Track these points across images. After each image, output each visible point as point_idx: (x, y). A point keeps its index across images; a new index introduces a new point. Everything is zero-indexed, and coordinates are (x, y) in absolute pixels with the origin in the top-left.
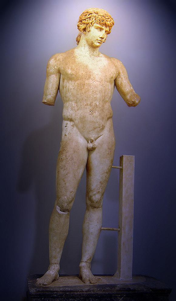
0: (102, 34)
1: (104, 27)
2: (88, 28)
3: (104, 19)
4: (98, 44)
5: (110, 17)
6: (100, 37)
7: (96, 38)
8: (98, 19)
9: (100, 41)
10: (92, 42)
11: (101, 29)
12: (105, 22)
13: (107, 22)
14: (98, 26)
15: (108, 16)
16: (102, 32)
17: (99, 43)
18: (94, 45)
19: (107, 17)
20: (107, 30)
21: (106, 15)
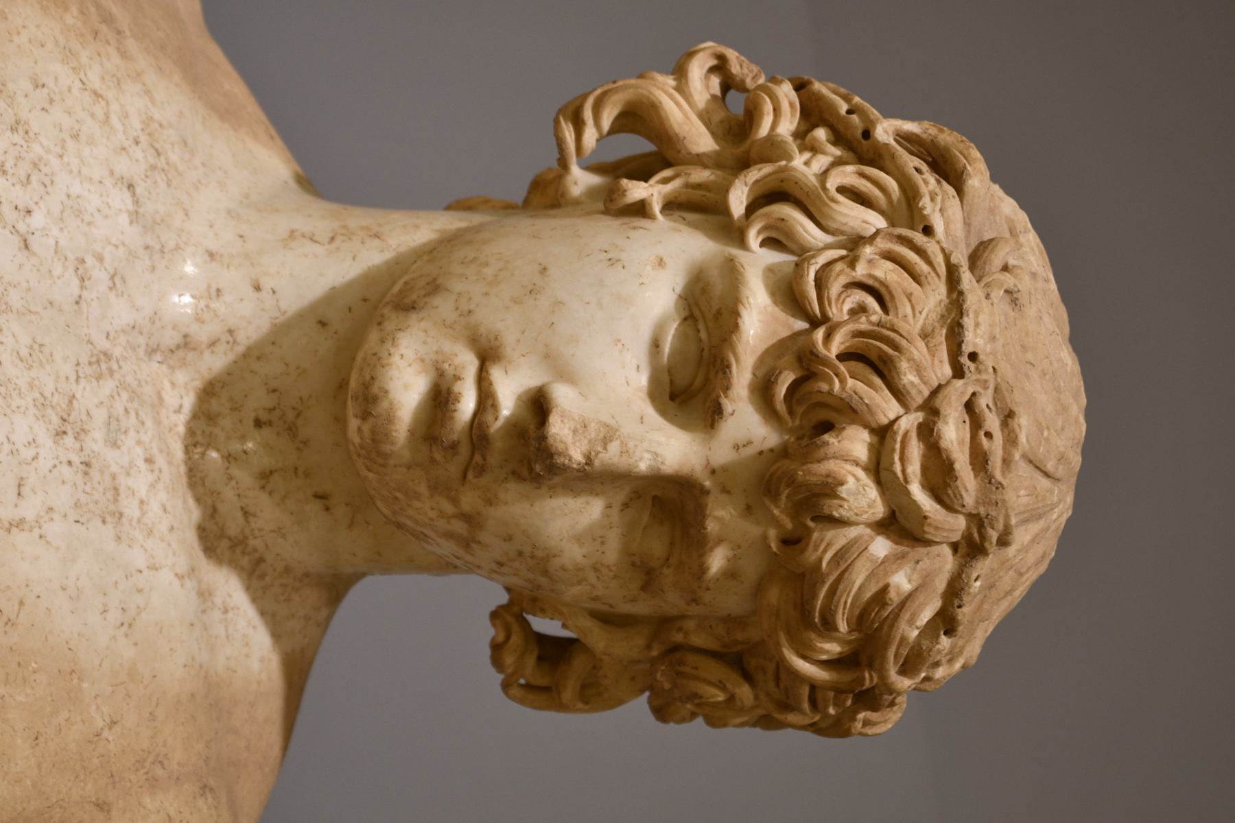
0: (611, 406)
1: (746, 426)
2: (669, 187)
3: (909, 378)
4: (406, 390)
5: (971, 548)
6: (563, 396)
7: (504, 324)
8: (886, 272)
9: (467, 405)
10: (434, 287)
11: (688, 389)
12: (851, 412)
13: (856, 443)
14: (759, 321)
15: (980, 460)
16: (650, 411)
17: (440, 399)
18: (373, 336)
19: (953, 433)
20: (721, 516)
21: (992, 422)
